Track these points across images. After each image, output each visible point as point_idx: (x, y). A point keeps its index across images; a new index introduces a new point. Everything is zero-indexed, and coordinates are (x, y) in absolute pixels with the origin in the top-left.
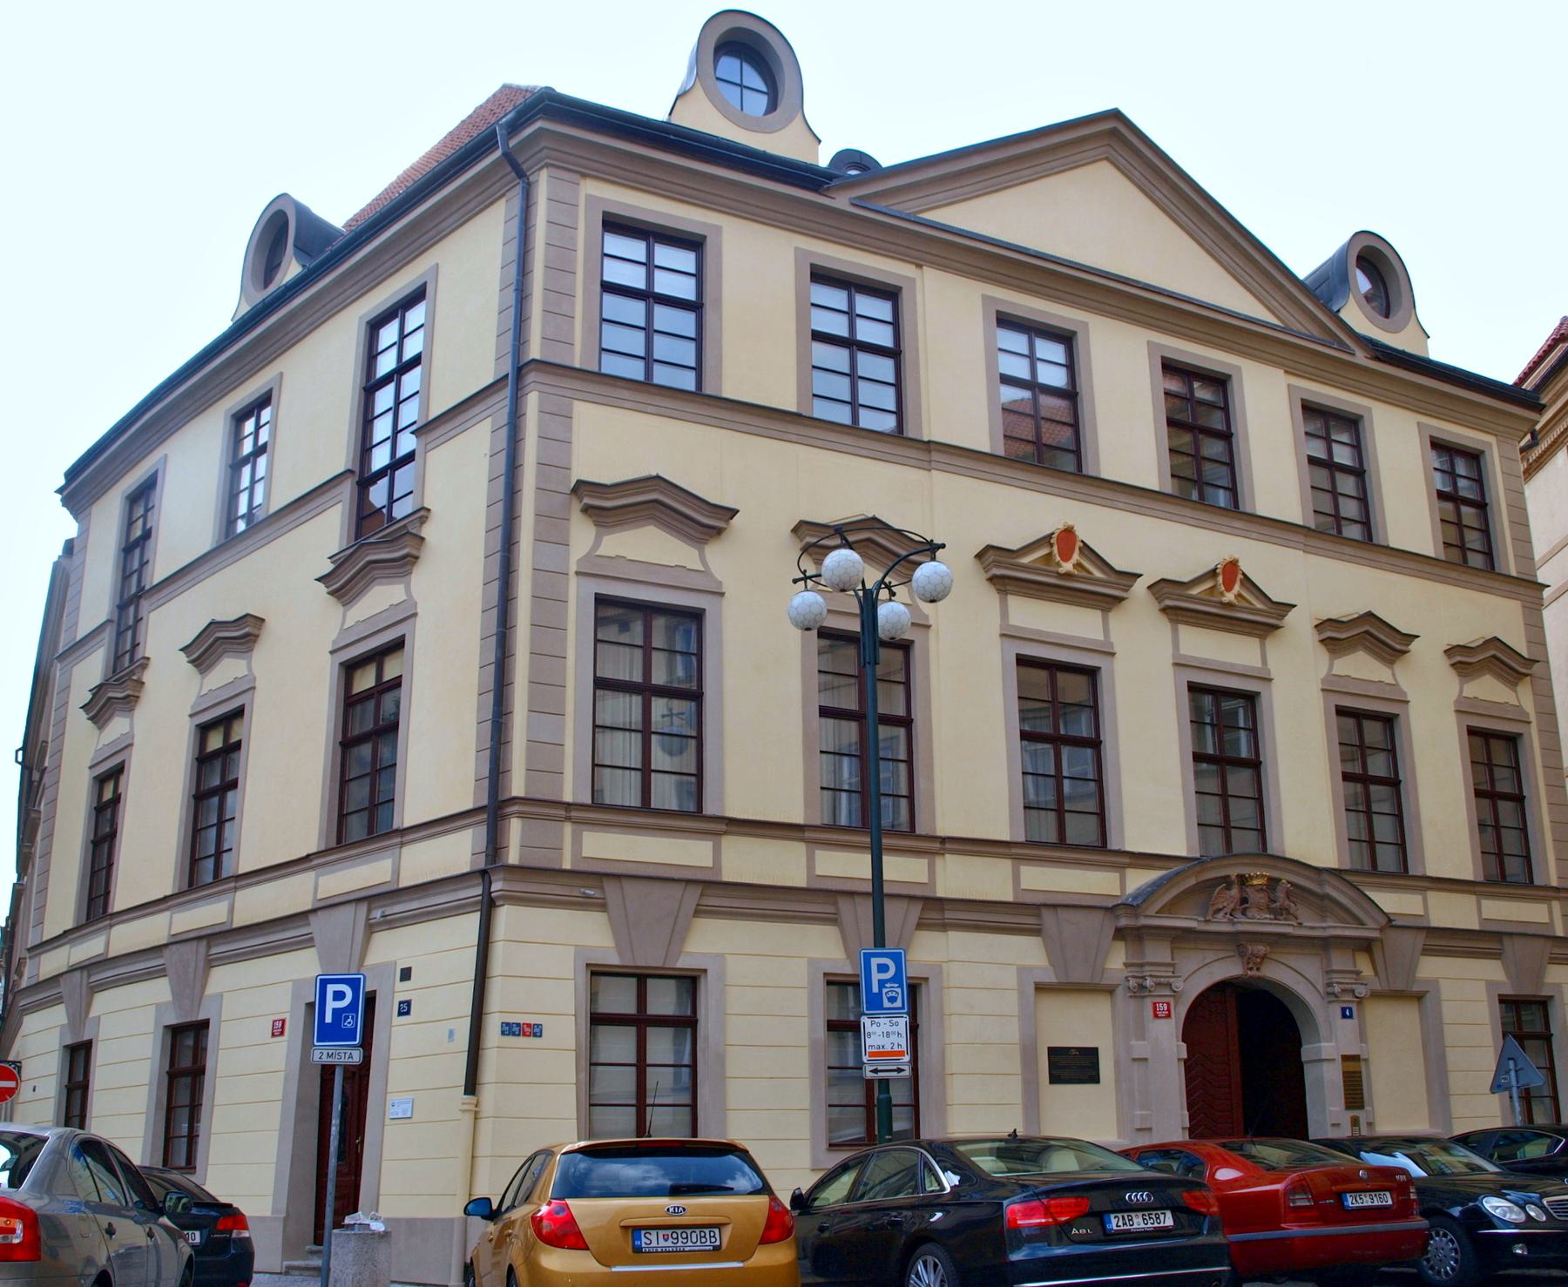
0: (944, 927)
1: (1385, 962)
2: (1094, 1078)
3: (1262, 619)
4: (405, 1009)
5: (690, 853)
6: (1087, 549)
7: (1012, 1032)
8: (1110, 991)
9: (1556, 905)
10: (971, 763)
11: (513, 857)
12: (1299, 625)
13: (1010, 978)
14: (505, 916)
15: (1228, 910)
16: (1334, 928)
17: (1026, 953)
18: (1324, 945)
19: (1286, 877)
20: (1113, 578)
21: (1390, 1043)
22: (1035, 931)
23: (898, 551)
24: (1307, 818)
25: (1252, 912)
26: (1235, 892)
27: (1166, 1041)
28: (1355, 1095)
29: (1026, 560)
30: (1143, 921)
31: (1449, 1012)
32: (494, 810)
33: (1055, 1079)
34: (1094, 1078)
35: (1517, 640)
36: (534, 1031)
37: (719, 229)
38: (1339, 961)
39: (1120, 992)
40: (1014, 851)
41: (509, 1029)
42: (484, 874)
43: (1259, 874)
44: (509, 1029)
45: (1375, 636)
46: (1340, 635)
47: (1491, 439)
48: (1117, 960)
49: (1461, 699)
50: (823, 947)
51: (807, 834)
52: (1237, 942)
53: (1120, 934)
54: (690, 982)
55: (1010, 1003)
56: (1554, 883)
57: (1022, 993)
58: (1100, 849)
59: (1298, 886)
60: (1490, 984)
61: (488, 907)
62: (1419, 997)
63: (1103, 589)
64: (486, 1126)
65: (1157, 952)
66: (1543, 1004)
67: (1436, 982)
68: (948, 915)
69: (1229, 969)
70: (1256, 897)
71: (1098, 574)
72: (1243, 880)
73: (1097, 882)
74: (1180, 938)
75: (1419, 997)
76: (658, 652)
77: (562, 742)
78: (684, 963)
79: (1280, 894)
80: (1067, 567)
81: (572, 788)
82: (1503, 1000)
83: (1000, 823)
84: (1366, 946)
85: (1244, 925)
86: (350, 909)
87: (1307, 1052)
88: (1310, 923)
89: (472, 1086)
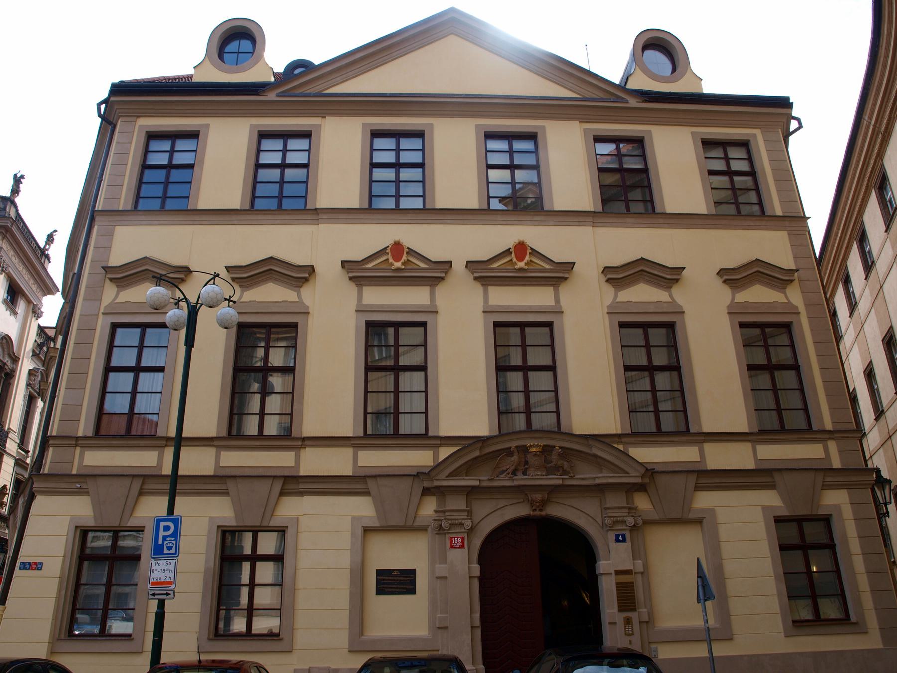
0: (301, 493)
2: (412, 591)
6: (411, 252)
7: (345, 560)
8: (423, 529)
13: (347, 525)
15: (510, 471)
16: (606, 477)
17: (362, 508)
18: (600, 489)
20: (433, 266)
22: (367, 493)
25: (531, 471)
26: (515, 458)
27: (462, 563)
29: (495, 265)
30: (436, 483)
31: (724, 532)
33: (379, 592)
34: (412, 591)
38: (615, 500)
39: (429, 529)
40: (352, 442)
43: (534, 444)
51: (215, 443)
53: (426, 491)
57: (353, 535)
59: (568, 451)
60: (765, 509)
65: (457, 503)
68: (301, 486)
69: (521, 511)
71: (422, 265)
72: (524, 449)
73: (421, 458)
79: (554, 457)
82: (778, 520)
83: (347, 426)
85: (521, 480)
88: (586, 474)
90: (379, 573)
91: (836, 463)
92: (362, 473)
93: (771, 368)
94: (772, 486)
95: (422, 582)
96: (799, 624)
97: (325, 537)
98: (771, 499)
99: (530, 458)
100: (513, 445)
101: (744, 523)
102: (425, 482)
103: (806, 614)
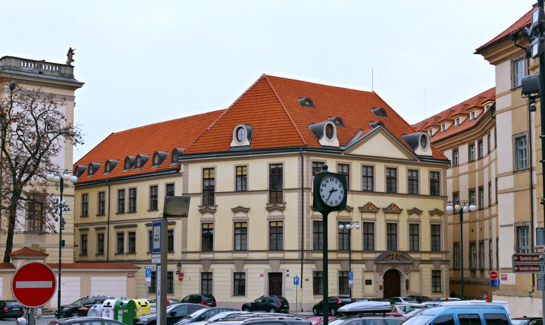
3: (399, 211)
4: (288, 275)
7: (361, 278)
8: (374, 272)
9: (444, 255)
10: (357, 240)
11: (305, 257)
12: (405, 212)
14: (304, 265)
17: (363, 266)
18: (404, 264)
19: (399, 254)
21: (414, 278)
24: (403, 244)
28: (407, 288)
31: (423, 273)
32: (302, 251)
37: (326, 161)
38: (407, 266)
41: (306, 280)
42: (302, 260)
43: (395, 254)
44: (306, 280)
45: (416, 211)
46: (410, 212)
47: (441, 169)
49: (430, 220)
53: (375, 263)
55: (361, 274)
56: (444, 250)
58: (373, 251)
61: (302, 264)
62: (419, 271)
64: (304, 292)
65: (381, 266)
66: (440, 271)
67: (421, 268)
70: (395, 257)
72: (393, 255)
75: (419, 271)
80: (371, 208)
81: (311, 248)
82: (433, 271)
84: (411, 264)
85: (393, 262)
87: (401, 280)
89: (301, 287)
90: (366, 280)
91: (444, 259)
95: (373, 282)
96: (433, 292)
97: (358, 272)
98: (431, 266)
100: (391, 254)
102: (376, 261)
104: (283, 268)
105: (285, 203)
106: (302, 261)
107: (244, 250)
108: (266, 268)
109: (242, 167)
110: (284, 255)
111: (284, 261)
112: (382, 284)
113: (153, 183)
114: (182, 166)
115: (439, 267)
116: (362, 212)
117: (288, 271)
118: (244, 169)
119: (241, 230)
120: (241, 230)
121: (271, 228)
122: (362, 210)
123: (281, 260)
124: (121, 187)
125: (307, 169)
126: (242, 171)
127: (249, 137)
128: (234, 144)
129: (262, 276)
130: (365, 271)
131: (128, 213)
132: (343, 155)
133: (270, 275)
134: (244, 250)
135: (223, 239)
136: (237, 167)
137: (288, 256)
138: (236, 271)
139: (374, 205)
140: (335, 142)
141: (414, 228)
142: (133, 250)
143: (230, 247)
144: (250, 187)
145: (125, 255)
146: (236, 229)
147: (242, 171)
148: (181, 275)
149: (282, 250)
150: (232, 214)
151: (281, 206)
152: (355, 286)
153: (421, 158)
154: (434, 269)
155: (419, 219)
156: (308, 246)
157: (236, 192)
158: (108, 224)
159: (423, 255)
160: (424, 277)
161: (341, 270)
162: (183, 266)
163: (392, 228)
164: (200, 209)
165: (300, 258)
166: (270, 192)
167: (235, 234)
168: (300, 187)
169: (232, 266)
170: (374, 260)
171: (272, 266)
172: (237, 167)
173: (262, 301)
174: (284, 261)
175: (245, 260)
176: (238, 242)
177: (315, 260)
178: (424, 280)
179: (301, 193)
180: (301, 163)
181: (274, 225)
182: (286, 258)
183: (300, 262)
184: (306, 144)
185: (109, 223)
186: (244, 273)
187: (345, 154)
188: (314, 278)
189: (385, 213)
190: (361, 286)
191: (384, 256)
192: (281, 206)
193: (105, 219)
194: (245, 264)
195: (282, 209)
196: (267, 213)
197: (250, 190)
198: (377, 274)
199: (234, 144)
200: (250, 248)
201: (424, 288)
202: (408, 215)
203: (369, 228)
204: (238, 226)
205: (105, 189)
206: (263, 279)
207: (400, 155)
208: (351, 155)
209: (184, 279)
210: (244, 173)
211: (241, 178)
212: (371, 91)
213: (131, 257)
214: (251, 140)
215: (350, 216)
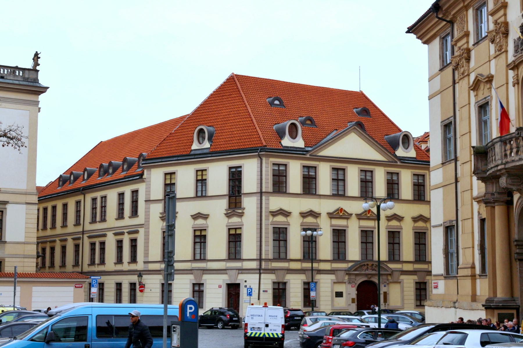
0: (320, 274)
1: (393, 277)
5: (284, 265)
7: (330, 289)
8: (345, 283)
10: (325, 248)
11: (263, 267)
14: (262, 275)
17: (332, 277)
23: (314, 214)
26: (366, 267)
28: (385, 300)
31: (405, 285)
32: (260, 260)
33: (336, 297)
35: (426, 215)
36: (266, 291)
41: (264, 291)
42: (260, 270)
43: (370, 263)
44: (264, 291)
48: (347, 277)
49: (414, 227)
50: (302, 278)
52: (366, 275)
53: (347, 274)
54: (285, 284)
55: (330, 285)
61: (260, 274)
62: (400, 282)
63: (347, 216)
65: (353, 277)
69: (364, 279)
70: (370, 268)
72: (367, 265)
74: (356, 275)
75: (400, 282)
76: (280, 235)
77: (269, 251)
78: (285, 281)
82: (416, 283)
84: (390, 274)
85: (367, 272)
86: (235, 271)
89: (259, 299)
90: (336, 292)
92: (333, 269)
93: (419, 244)
94: (416, 275)
95: (344, 294)
96: (417, 306)
98: (415, 277)
99: (369, 267)
100: (366, 263)
101: (409, 283)
102: (348, 272)
103: (419, 304)
104: (241, 278)
105: (244, 209)
106: (260, 271)
107: (203, 259)
108: (223, 279)
109: (202, 171)
110: (242, 265)
111: (241, 271)
112: (355, 296)
113: (120, 190)
114: (145, 171)
115: (424, 278)
116: (331, 218)
117: (246, 281)
118: (204, 173)
119: (200, 238)
120: (200, 238)
121: (230, 235)
122: (331, 216)
123: (239, 270)
124: (94, 195)
125: (267, 171)
126: (202, 175)
127: (210, 139)
128: (195, 146)
129: (220, 287)
130: (334, 283)
131: (99, 222)
132: (308, 156)
133: (229, 286)
134: (203, 259)
135: (183, 247)
136: (197, 171)
137: (247, 265)
138: (194, 282)
139: (345, 211)
140: (299, 143)
141: (394, 237)
142: (102, 262)
143: (190, 257)
144: (210, 193)
145: (96, 266)
146: (195, 236)
147: (202, 175)
148: (142, 286)
149: (240, 259)
150: (191, 222)
151: (240, 211)
152: (322, 299)
153: (402, 159)
154: (417, 281)
155: (401, 226)
156: (267, 254)
157: (197, 197)
158: (83, 234)
159: (404, 265)
160: (405, 289)
161: (306, 281)
162: (144, 277)
163: (367, 237)
164: (161, 216)
165: (258, 267)
166: (230, 197)
167: (195, 243)
168: (259, 191)
169: (191, 277)
170: (345, 270)
171: (230, 277)
172: (197, 171)
173: (211, 313)
174: (241, 271)
175: (204, 270)
176: (198, 251)
177: (274, 270)
178: (405, 293)
179: (259, 198)
180: (259, 164)
181: (232, 232)
182: (244, 268)
183: (258, 271)
184: (264, 144)
185: (83, 232)
186: (203, 284)
187: (310, 155)
188: (274, 289)
189: (359, 219)
190: (330, 298)
191: (358, 266)
192: (240, 211)
193: (80, 229)
194: (203, 274)
195: (241, 215)
196: (226, 219)
197: (209, 195)
198: (350, 286)
199: (195, 146)
200: (209, 256)
201: (406, 302)
202: (387, 222)
203: (339, 236)
204: (198, 233)
205: (81, 198)
206: (221, 289)
207: (377, 156)
208: (318, 156)
209: (146, 290)
210: (204, 178)
211: (201, 181)
212: (358, 91)
213: (101, 268)
214: (212, 142)
215: (317, 223)
